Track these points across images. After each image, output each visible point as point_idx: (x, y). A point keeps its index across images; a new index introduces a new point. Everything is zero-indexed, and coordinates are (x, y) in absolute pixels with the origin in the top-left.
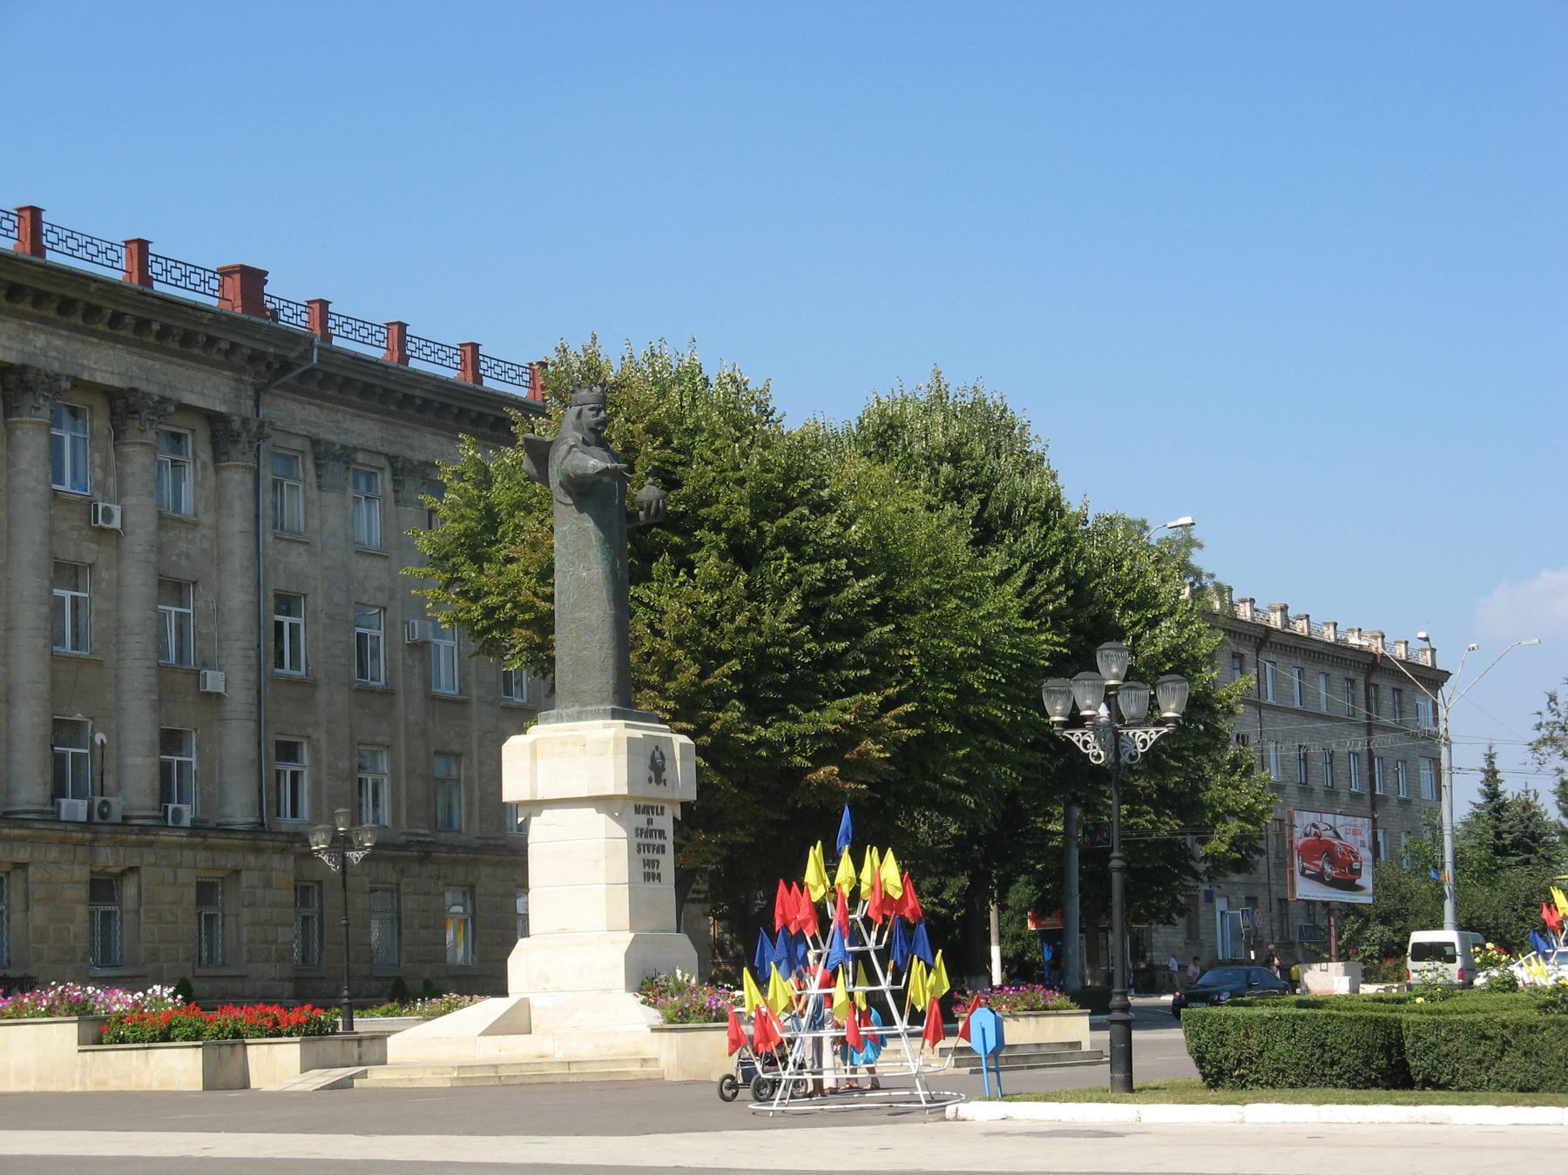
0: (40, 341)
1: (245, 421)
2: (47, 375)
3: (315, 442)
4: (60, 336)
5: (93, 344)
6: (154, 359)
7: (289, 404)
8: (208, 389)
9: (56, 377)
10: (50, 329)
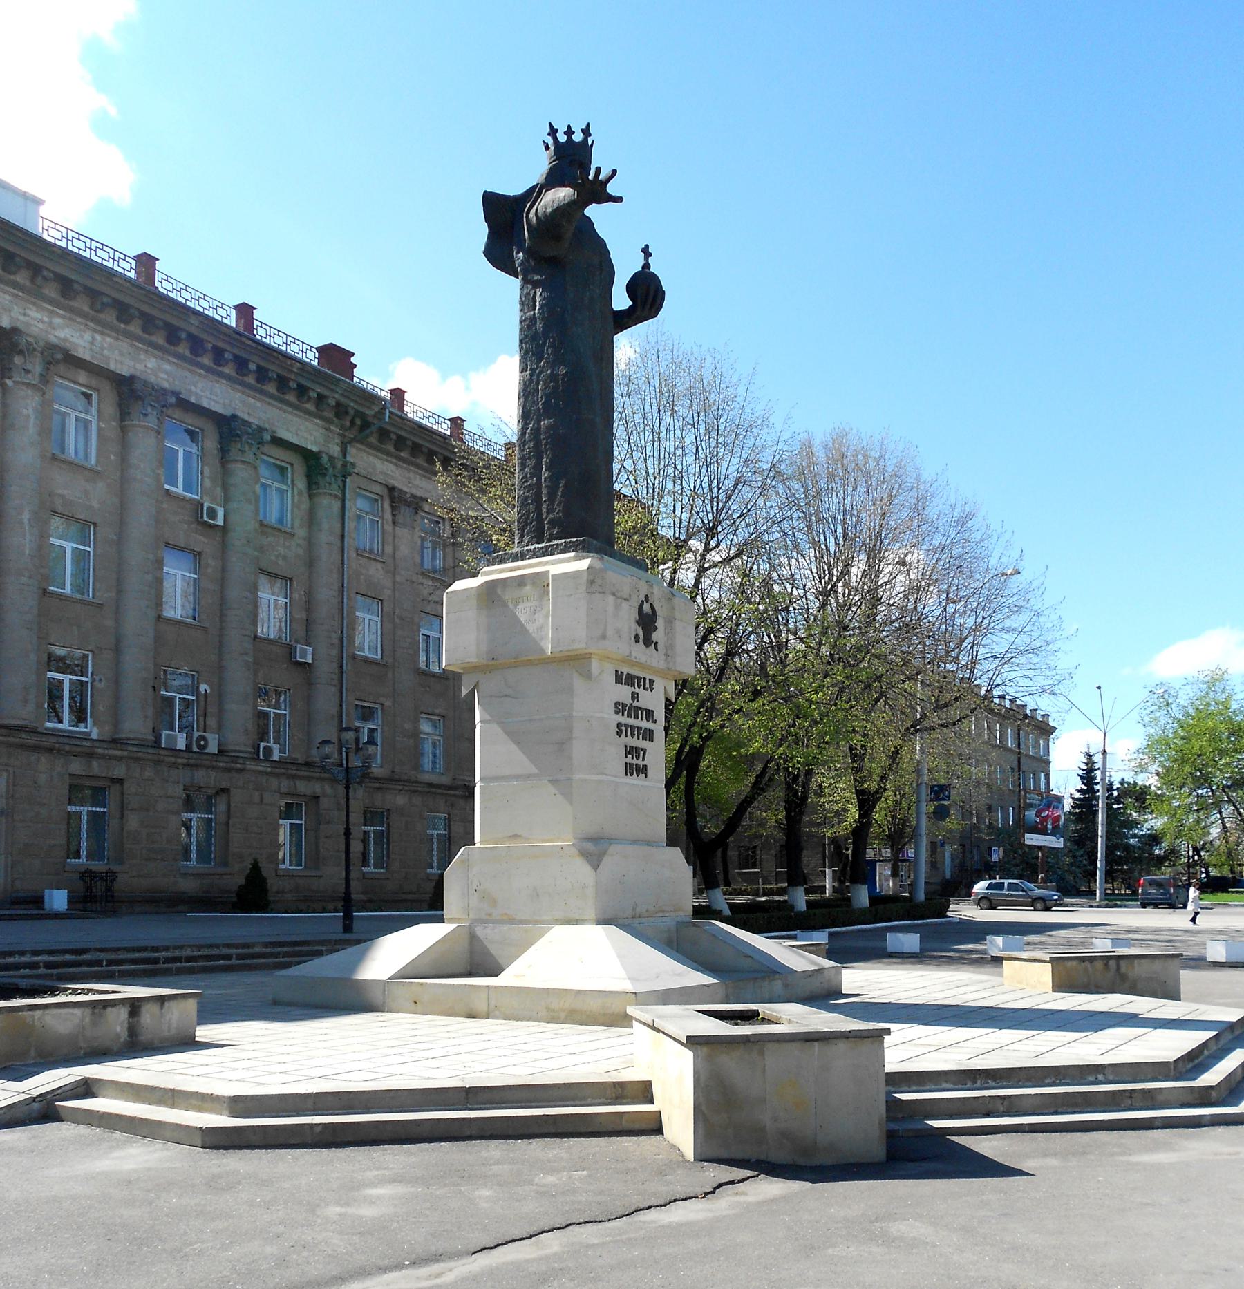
0: (152, 363)
1: (331, 458)
3: (391, 489)
4: (170, 362)
5: (200, 375)
7: (371, 459)
8: (306, 431)
9: (164, 392)
10: (160, 354)
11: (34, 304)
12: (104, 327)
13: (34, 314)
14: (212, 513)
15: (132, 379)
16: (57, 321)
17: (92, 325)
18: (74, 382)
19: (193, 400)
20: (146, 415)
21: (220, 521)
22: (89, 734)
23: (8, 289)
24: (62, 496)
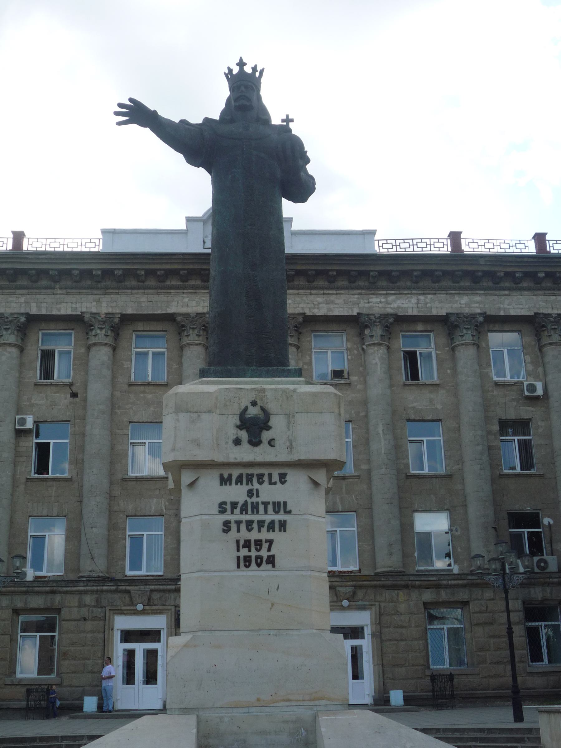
0: (465, 300)
2: (467, 317)
4: (479, 295)
5: (505, 295)
6: (555, 295)
9: (473, 316)
11: (374, 294)
13: (374, 299)
14: (532, 388)
15: (448, 315)
16: (391, 298)
17: (415, 292)
18: (416, 331)
19: (502, 313)
20: (463, 336)
21: (540, 392)
22: (452, 570)
23: (355, 292)
24: (413, 408)
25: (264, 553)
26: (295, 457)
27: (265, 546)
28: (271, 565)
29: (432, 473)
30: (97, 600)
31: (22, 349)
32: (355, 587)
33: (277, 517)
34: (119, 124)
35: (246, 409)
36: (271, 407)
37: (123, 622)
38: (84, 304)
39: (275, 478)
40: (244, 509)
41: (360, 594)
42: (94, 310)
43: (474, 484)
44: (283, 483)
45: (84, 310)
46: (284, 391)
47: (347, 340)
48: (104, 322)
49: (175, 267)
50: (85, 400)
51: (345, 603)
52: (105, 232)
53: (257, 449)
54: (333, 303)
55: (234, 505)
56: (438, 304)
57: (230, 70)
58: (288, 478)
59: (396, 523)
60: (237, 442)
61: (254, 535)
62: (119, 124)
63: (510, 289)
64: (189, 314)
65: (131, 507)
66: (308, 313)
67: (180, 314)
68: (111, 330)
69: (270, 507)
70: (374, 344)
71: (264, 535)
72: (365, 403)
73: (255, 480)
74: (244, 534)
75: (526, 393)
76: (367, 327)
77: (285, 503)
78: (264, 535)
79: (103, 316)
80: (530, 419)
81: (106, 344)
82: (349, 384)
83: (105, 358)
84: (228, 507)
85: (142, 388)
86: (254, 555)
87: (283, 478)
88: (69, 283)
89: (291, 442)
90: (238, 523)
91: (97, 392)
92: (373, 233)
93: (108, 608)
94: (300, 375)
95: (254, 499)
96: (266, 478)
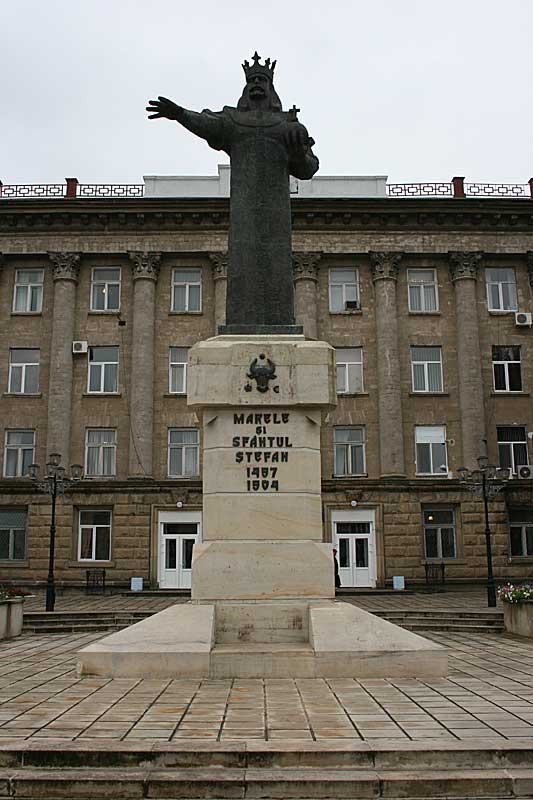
0: (465, 239)
5: (501, 235)
9: (473, 254)
12: (429, 230)
14: (523, 318)
19: (498, 251)
22: (446, 476)
24: (417, 335)
25: (269, 479)
26: (295, 402)
27: (270, 473)
28: (274, 490)
29: (432, 392)
30: (143, 499)
31: (76, 284)
32: (363, 490)
33: (280, 450)
34: (151, 117)
35: (256, 360)
36: (276, 360)
37: (166, 517)
38: (129, 244)
39: (279, 418)
40: (253, 443)
41: (366, 495)
42: (138, 249)
43: (469, 402)
44: (285, 422)
45: (129, 249)
46: (287, 346)
47: (360, 275)
48: (147, 260)
49: (208, 210)
50: (131, 328)
51: (354, 503)
52: (145, 179)
53: (264, 395)
54: (348, 242)
55: (245, 440)
56: (442, 244)
57: (247, 63)
58: (289, 418)
59: (399, 436)
60: (248, 389)
61: (261, 464)
62: (151, 117)
63: (506, 230)
64: (221, 253)
65: (171, 419)
66: (325, 252)
67: (213, 253)
68: (154, 267)
69: (275, 441)
70: (383, 279)
71: (270, 464)
72: (374, 330)
73: (262, 420)
74: (253, 463)
75: (517, 323)
76: (377, 263)
77: (287, 438)
78: (270, 464)
79: (146, 254)
80: (520, 346)
81: (149, 279)
82: (361, 314)
83: (148, 291)
84: (241, 441)
85: (180, 318)
86: (261, 481)
87: (285, 419)
88: (116, 225)
89: (292, 389)
90: (249, 454)
91: (142, 321)
92: (385, 178)
93: (153, 506)
94: (301, 333)
95: (262, 435)
96: (272, 418)
